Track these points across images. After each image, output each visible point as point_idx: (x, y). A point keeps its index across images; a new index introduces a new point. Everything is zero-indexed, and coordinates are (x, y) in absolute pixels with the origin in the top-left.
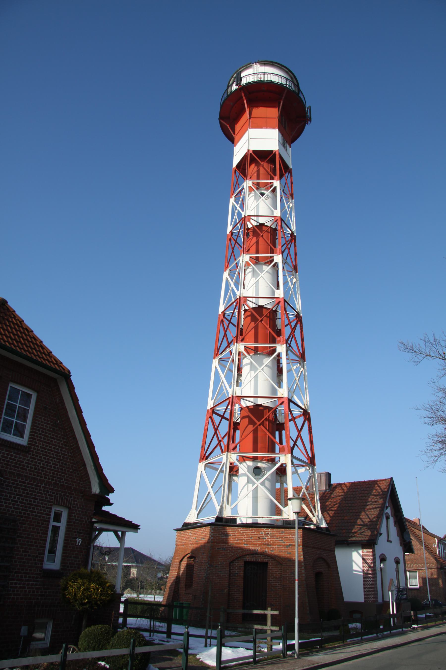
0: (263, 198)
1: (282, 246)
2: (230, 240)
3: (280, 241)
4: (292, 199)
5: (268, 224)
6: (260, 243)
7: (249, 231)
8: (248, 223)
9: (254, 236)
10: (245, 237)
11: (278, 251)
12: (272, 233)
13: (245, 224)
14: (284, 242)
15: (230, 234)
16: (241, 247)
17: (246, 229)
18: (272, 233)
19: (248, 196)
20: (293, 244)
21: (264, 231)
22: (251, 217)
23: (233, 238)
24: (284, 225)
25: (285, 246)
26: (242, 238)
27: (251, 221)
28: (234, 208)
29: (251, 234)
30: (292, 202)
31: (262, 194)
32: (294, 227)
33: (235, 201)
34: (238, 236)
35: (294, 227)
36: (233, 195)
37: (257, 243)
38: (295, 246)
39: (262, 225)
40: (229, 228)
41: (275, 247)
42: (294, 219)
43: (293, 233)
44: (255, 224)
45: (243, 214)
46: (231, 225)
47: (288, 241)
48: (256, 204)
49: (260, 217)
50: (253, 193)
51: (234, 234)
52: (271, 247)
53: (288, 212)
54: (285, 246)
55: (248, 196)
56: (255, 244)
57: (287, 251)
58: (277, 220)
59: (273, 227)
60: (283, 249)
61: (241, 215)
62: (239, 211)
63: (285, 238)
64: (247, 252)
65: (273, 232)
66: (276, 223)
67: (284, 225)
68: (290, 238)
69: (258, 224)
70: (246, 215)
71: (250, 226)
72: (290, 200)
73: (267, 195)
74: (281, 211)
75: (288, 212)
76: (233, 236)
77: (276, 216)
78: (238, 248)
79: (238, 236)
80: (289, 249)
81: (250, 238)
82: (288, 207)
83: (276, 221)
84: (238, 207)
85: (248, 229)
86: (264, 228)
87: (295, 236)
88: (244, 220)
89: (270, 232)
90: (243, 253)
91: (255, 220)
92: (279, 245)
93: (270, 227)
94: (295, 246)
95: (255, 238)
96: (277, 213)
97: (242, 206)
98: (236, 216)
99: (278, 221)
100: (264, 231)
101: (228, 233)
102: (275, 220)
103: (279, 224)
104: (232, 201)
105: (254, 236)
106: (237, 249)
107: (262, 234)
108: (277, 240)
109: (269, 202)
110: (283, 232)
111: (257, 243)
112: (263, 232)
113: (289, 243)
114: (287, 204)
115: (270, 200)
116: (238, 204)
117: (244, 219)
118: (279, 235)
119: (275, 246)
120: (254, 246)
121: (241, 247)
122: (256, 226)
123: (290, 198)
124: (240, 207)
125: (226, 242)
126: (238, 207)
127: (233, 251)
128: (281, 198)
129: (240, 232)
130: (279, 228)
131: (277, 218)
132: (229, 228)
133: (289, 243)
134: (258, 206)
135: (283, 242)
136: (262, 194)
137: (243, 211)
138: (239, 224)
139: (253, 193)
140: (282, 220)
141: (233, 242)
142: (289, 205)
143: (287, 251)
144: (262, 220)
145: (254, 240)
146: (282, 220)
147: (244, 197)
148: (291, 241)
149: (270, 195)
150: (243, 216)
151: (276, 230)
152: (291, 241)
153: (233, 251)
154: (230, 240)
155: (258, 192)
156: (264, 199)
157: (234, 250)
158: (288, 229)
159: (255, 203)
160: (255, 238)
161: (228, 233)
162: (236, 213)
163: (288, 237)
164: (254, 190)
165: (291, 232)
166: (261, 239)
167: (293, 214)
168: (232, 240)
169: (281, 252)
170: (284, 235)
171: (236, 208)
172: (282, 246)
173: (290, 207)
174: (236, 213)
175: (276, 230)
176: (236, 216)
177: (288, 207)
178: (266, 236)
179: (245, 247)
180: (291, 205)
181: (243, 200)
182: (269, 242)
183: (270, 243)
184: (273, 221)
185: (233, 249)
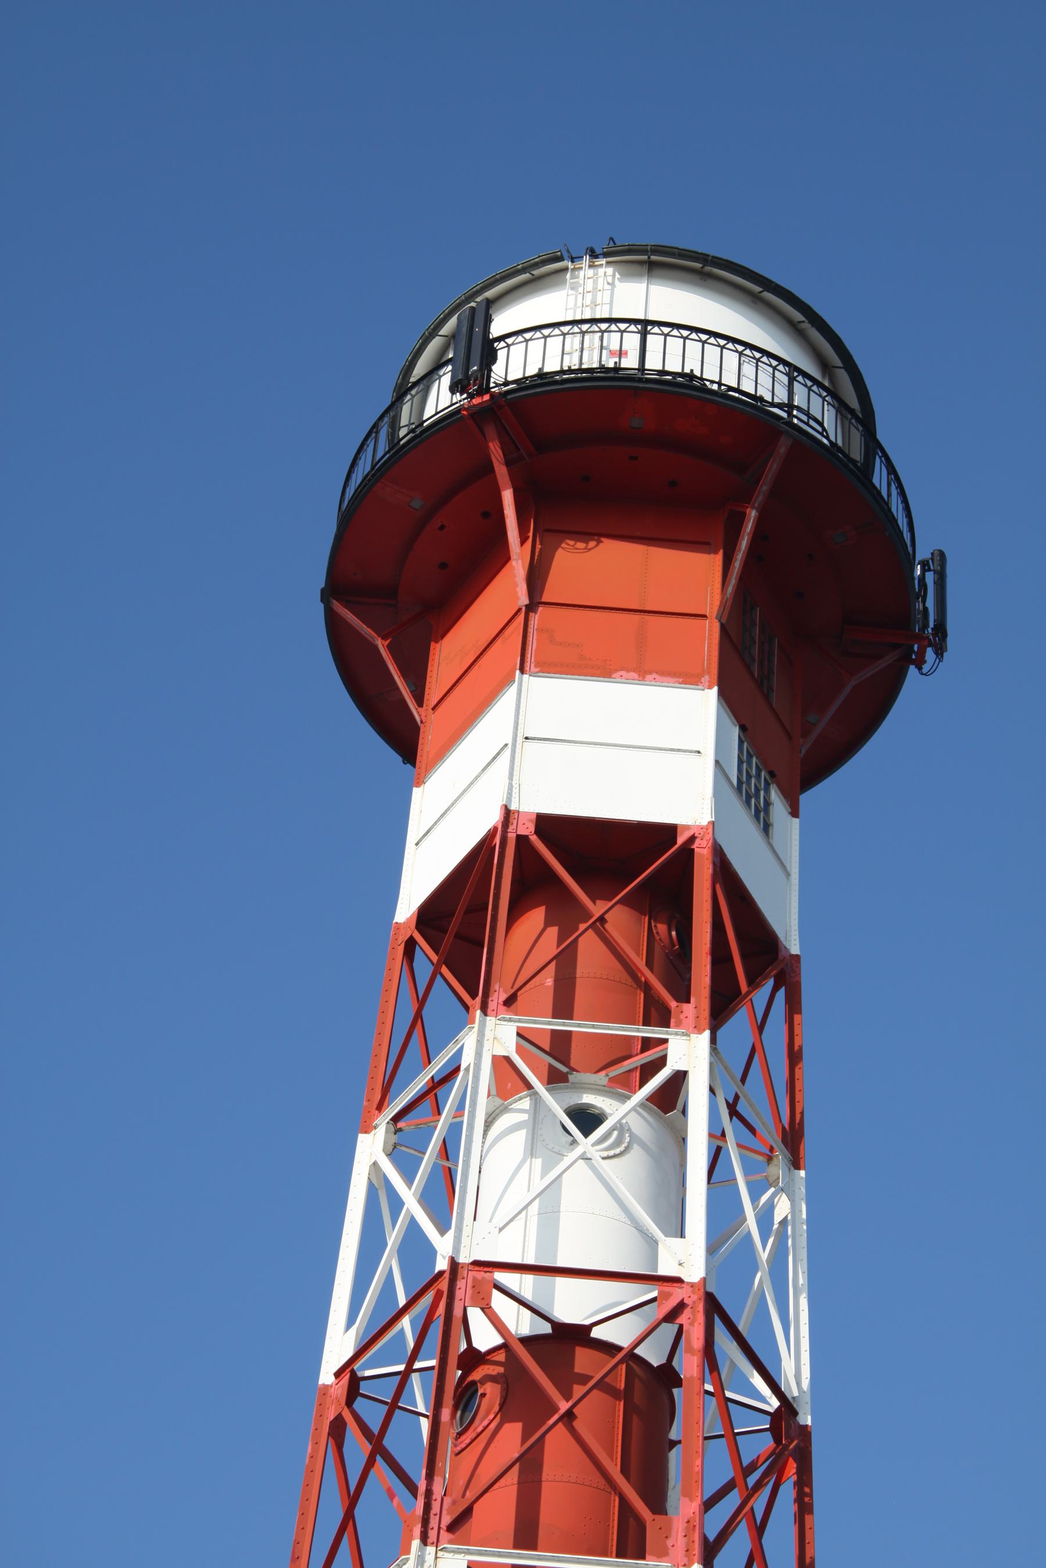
0: (586, 1144)
1: (708, 1504)
2: (337, 1430)
3: (696, 1467)
4: (796, 1163)
5: (618, 1333)
6: (549, 1471)
7: (476, 1375)
8: (475, 1316)
9: (506, 1411)
10: (446, 1414)
11: (678, 1540)
12: (638, 1398)
13: (453, 1324)
14: (727, 1473)
15: (340, 1391)
16: (413, 1489)
17: (453, 1360)
18: (638, 1398)
19: (488, 1125)
20: (787, 1491)
21: (584, 1379)
22: (501, 1277)
23: (355, 1418)
24: (725, 1345)
25: (733, 1499)
26: (425, 1424)
27: (499, 1302)
28: (381, 1200)
29: (491, 1393)
30: (788, 1190)
31: (587, 1120)
32: (796, 1369)
33: (393, 1152)
34: (393, 1406)
35: (796, 1369)
36: (380, 1107)
37: (530, 1463)
38: (804, 1507)
39: (570, 1337)
40: (339, 1345)
41: (658, 1503)
42: (802, 1308)
43: (787, 1408)
44: (522, 1324)
45: (443, 1247)
46: (350, 1322)
47: (753, 1467)
48: (539, 1185)
49: (561, 1281)
50: (525, 1104)
51: (364, 1388)
52: (625, 1505)
53: (764, 1255)
54: (733, 1499)
55: (488, 1125)
56: (513, 1475)
57: (740, 1542)
58: (681, 1306)
59: (653, 1354)
60: (713, 1526)
61: (432, 1252)
62: (413, 1223)
63: (732, 1437)
64: (452, 1528)
65: (648, 1389)
66: (668, 1331)
67: (725, 1345)
68: (767, 1442)
69: (546, 1329)
70: (464, 1259)
71: (484, 1337)
72: (779, 1168)
73: (620, 1127)
74: (712, 1249)
75: (764, 1255)
76: (359, 1404)
77: (678, 1280)
78: (391, 1495)
79: (393, 1406)
80: (759, 1530)
81: (478, 1426)
82: (765, 1217)
83: (670, 1317)
84: (409, 1197)
85: (473, 1358)
86: (583, 1359)
87: (805, 1432)
88: (446, 1292)
89: (627, 1396)
90: (424, 1540)
91: (528, 1295)
92: (687, 1493)
93: (631, 1357)
94: (804, 1507)
95: (513, 1431)
96: (686, 1258)
97: (443, 1194)
98: (389, 1261)
99: (683, 1319)
100: (584, 1379)
101: (327, 1377)
102: (672, 1303)
103: (696, 1335)
104: (371, 1148)
105: (506, 1411)
106: (382, 1504)
107: (564, 1406)
108: (674, 1456)
109: (628, 1173)
110: (719, 1393)
111: (530, 1463)
112: (578, 1390)
113: (759, 1485)
114: (755, 1198)
115: (635, 1159)
116: (409, 1180)
117: (444, 1285)
118: (692, 1415)
119: (656, 1498)
120: (507, 1494)
121: (413, 1489)
122: (525, 1341)
123: (781, 1157)
124: (425, 1200)
125: (307, 1442)
126: (409, 1197)
127: (349, 1517)
128: (716, 1156)
129: (415, 1378)
130: (688, 1365)
131: (678, 1294)
132: (339, 1345)
133: (759, 1485)
134: (549, 1195)
135: (719, 1469)
136: (587, 1120)
137: (443, 1230)
138: (406, 1322)
139: (525, 1104)
140: (713, 1306)
141: (356, 1449)
142: (770, 1206)
143: (740, 1542)
144: (573, 1303)
145: (511, 1441)
146: (713, 1306)
147: (455, 1129)
148: (776, 1469)
149: (641, 1125)
150: (442, 1264)
151: (667, 1376)
152: (776, 1469)
153: (349, 1517)
154: (337, 1430)
155: (555, 1104)
156: (595, 1153)
157: (357, 1512)
158: (758, 1381)
159: (534, 1177)
160: (513, 1431)
161: (327, 1377)
162: (393, 1237)
163: (758, 1446)
164: (529, 1086)
165: (775, 1403)
166: (557, 1443)
167: (798, 1274)
168: (353, 1437)
169: (697, 1549)
170: (728, 1421)
171: (396, 1203)
172: (708, 1504)
173: (778, 1218)
174: (393, 1237)
175: (667, 1376)
176: (389, 1261)
177: (765, 1217)
178: (598, 1417)
179: (438, 1489)
180: (782, 1208)
181: (447, 1151)
182: (614, 1469)
183: (625, 1471)
184: (654, 1313)
185: (352, 1500)
